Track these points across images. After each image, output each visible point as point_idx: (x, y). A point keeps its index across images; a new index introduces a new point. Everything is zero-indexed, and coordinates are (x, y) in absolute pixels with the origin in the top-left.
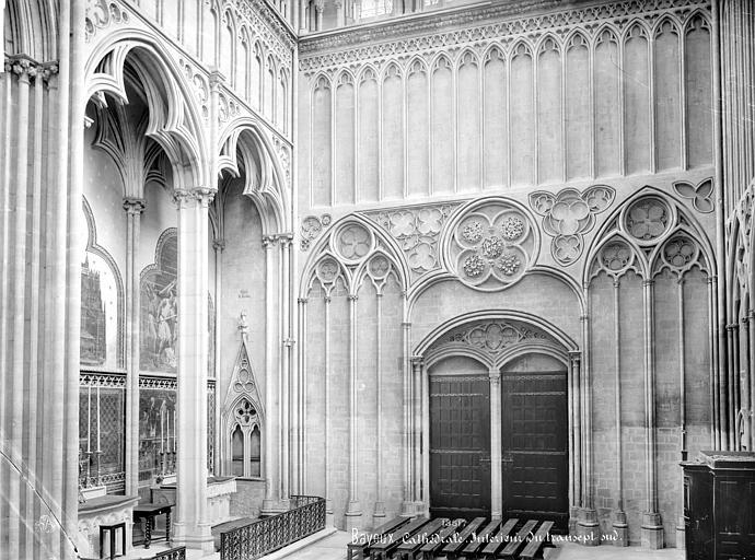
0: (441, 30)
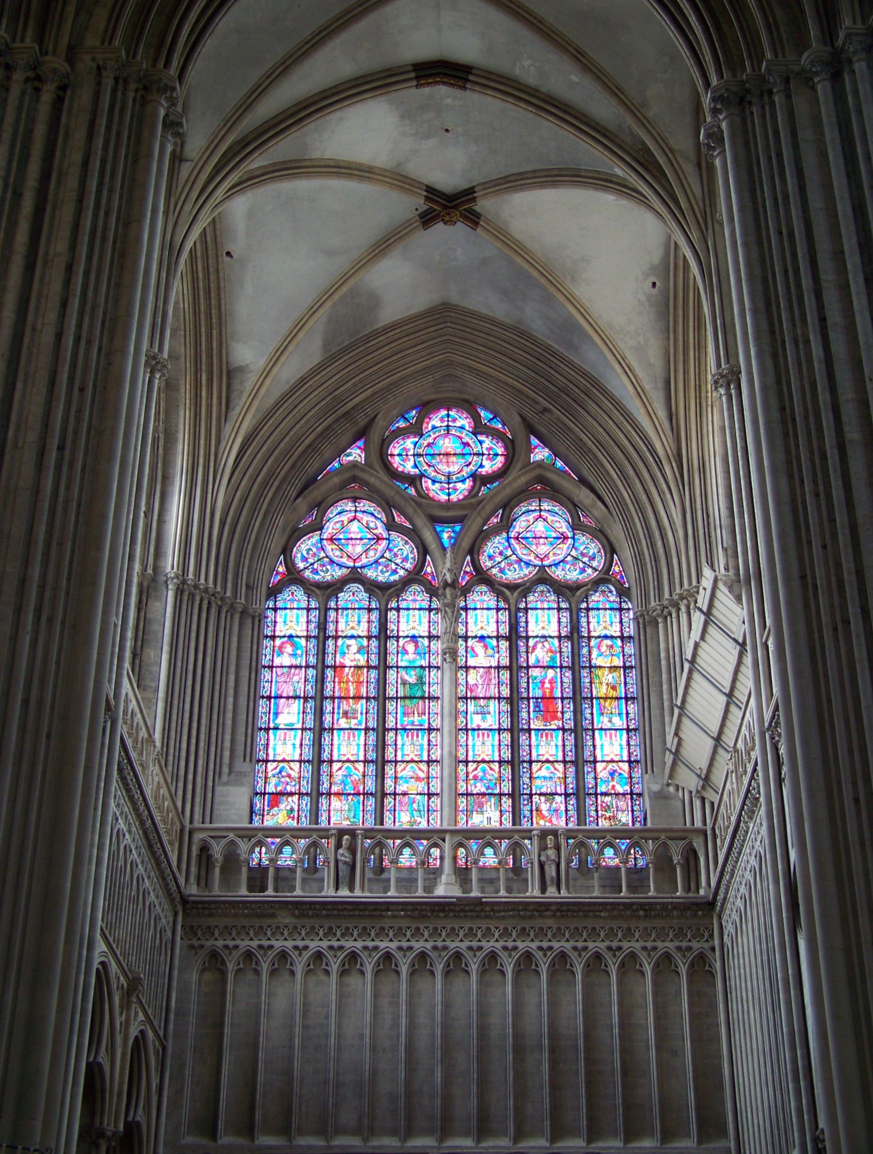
0: (387, 920)
